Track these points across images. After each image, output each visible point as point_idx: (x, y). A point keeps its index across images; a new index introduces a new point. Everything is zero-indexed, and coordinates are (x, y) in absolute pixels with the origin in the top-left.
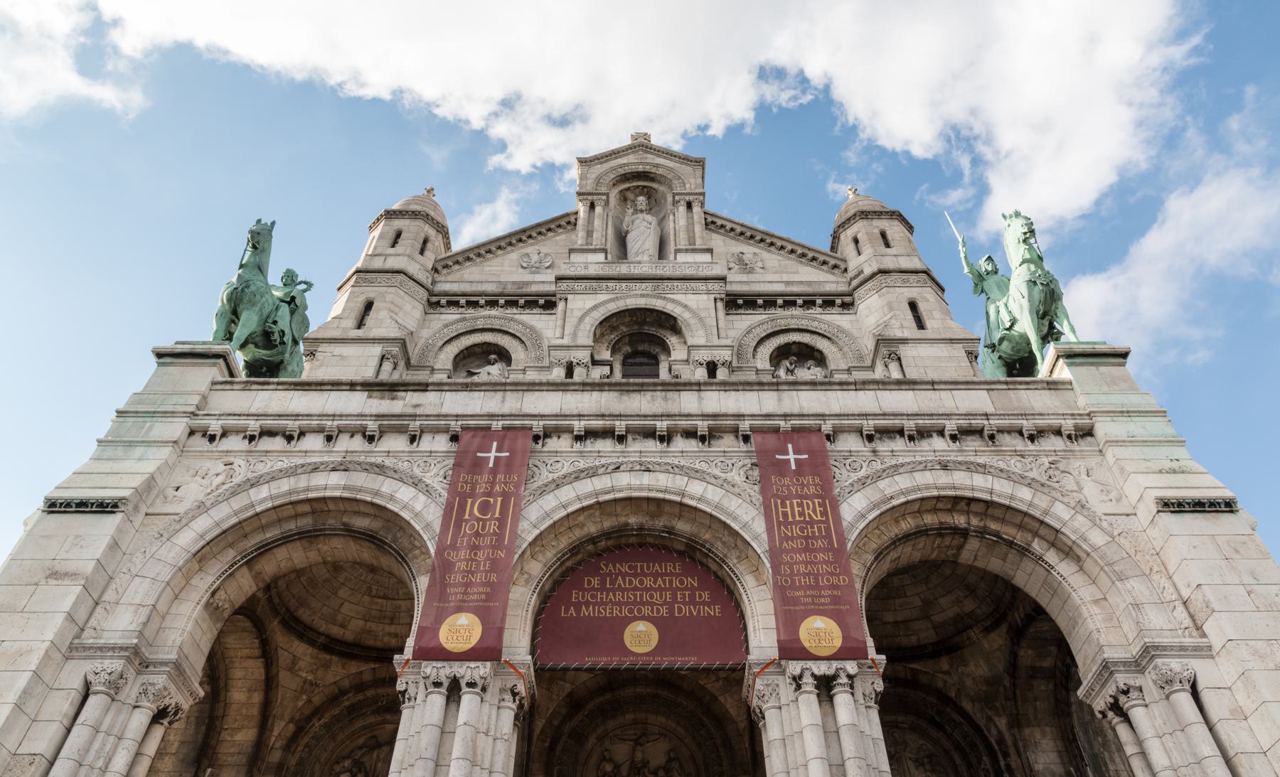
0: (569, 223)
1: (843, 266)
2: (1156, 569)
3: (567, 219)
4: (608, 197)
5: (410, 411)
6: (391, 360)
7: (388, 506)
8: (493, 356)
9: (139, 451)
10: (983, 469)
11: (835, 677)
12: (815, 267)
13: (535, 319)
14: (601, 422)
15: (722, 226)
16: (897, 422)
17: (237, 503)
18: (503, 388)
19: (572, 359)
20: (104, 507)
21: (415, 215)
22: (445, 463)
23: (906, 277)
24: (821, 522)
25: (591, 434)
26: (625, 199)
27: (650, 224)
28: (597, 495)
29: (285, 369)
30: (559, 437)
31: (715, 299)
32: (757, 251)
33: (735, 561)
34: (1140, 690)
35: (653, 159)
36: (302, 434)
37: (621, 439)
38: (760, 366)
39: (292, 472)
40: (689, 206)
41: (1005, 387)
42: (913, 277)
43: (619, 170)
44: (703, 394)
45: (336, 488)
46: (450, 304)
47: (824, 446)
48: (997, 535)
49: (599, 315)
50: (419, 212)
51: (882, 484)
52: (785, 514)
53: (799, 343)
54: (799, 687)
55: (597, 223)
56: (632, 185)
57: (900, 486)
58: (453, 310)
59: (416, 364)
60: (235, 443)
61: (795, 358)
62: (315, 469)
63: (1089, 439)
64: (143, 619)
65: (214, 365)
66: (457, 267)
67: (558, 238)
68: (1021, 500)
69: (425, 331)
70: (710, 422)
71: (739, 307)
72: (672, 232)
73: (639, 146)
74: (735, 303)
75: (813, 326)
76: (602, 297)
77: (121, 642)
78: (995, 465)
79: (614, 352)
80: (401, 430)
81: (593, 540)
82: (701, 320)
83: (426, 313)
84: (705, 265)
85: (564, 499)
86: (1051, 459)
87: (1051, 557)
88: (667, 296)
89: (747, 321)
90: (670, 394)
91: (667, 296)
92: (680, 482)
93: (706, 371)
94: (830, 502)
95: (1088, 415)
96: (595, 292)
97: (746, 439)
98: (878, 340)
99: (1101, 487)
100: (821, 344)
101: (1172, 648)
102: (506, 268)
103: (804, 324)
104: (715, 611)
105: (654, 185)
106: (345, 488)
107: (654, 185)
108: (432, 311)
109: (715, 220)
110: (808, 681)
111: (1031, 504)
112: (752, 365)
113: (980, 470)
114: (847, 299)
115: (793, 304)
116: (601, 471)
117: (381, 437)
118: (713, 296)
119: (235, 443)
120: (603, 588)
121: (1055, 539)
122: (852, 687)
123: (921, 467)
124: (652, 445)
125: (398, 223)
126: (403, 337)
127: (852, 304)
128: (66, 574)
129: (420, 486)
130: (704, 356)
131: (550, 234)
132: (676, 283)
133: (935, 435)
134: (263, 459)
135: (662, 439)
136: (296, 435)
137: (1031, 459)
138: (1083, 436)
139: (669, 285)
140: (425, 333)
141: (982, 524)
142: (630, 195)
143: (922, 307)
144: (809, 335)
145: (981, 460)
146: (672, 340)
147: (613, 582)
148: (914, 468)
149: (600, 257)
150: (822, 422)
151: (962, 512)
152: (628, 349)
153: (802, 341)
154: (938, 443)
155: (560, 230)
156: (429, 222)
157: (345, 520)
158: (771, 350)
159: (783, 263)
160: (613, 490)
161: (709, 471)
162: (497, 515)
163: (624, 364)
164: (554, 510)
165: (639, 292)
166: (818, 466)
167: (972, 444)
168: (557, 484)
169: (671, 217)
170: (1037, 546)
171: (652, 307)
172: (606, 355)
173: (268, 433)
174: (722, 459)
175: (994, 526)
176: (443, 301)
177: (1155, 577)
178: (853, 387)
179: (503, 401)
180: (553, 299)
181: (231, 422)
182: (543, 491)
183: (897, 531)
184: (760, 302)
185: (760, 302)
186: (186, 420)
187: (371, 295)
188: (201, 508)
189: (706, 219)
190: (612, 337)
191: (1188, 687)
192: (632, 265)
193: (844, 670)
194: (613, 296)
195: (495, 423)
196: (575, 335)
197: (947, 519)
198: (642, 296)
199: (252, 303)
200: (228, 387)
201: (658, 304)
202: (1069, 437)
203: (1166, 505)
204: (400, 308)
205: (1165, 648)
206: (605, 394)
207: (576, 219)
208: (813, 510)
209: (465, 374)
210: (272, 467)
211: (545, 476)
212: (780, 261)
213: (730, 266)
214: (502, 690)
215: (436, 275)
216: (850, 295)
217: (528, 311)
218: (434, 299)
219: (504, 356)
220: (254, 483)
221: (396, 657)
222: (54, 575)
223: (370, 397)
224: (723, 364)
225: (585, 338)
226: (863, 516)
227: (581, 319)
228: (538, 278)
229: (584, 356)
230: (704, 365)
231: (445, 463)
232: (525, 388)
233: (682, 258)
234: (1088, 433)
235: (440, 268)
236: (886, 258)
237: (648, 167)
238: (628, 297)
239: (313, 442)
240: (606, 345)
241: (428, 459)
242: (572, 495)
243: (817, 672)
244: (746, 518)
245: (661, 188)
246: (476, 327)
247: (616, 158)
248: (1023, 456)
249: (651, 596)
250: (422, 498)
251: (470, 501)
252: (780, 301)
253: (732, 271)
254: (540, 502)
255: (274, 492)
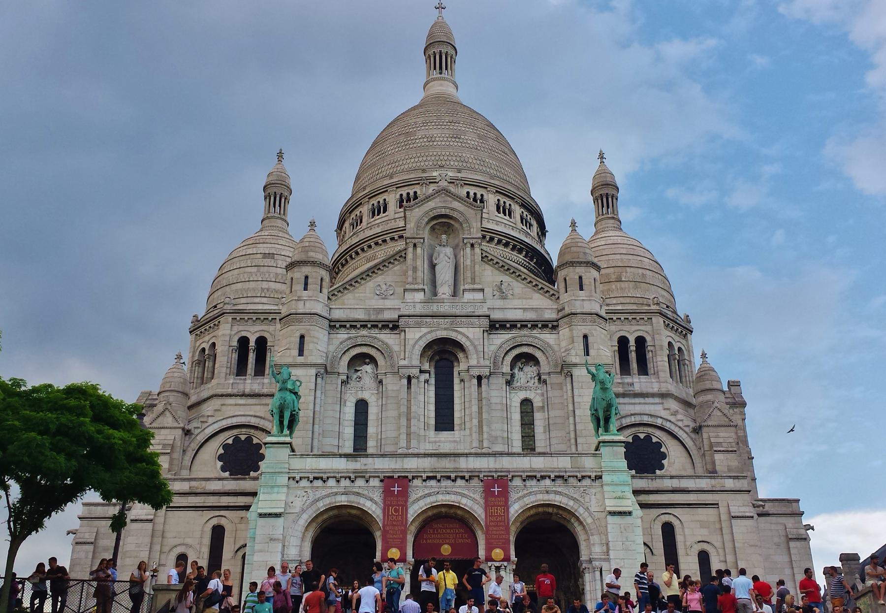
0: (401, 256)
1: (557, 296)
2: (603, 532)
3: (399, 255)
4: (424, 241)
5: (363, 467)
6: (321, 376)
7: (364, 508)
8: (367, 360)
9: (276, 490)
10: (560, 493)
11: (501, 566)
12: (541, 294)
13: (387, 338)
14: (432, 474)
15: (492, 260)
16: (534, 474)
17: (314, 508)
18: (395, 456)
19: (411, 374)
20: (277, 515)
21: (314, 263)
22: (380, 490)
23: (584, 318)
24: (503, 516)
25: (429, 478)
26: (434, 229)
27: (449, 259)
28: (431, 503)
29: (295, 421)
30: (417, 479)
31: (483, 331)
32: (510, 279)
33: (476, 525)
34: (589, 568)
35: (451, 202)
36: (328, 478)
37: (439, 481)
38: (504, 370)
39: (328, 496)
40: (472, 245)
41: (577, 455)
42: (589, 317)
43: (431, 213)
44: (468, 458)
45: (345, 502)
46: (341, 326)
47: (508, 483)
48: (561, 515)
49: (423, 343)
50: (316, 262)
51: (525, 499)
52: (492, 512)
53: (527, 353)
54: (490, 569)
55: (419, 263)
56: (438, 221)
57: (531, 501)
58: (343, 330)
59: (330, 371)
60: (304, 483)
61: (524, 360)
62: (336, 494)
63: (600, 480)
64: (298, 551)
65: (287, 447)
66: (340, 294)
67: (395, 268)
68: (569, 506)
69: (331, 346)
70: (470, 474)
71: (497, 329)
72: (462, 267)
73: (442, 190)
74: (495, 326)
75: (535, 342)
76: (424, 330)
77: (296, 559)
78: (564, 492)
79: (430, 361)
80: (364, 477)
81: (430, 517)
82: (475, 347)
83: (329, 334)
84: (479, 304)
85: (421, 506)
86: (584, 489)
87: (576, 524)
88: (458, 329)
89: (501, 338)
90: (457, 459)
91: (458, 329)
92: (459, 498)
93: (476, 380)
94: (506, 507)
95: (601, 471)
96: (419, 326)
97: (482, 481)
98: (563, 364)
99: (597, 501)
100: (538, 354)
101: (598, 559)
102: (368, 295)
103: (529, 341)
104: (469, 541)
105: (452, 222)
106: (348, 501)
107: (452, 222)
108: (332, 332)
109: (488, 255)
110: (493, 567)
111: (572, 507)
112: (500, 371)
113: (559, 494)
114: (555, 323)
115: (526, 326)
116: (432, 494)
117: (355, 479)
118: (482, 329)
119: (304, 483)
120: (434, 533)
121: (578, 519)
122: (505, 569)
123: (540, 492)
124: (449, 483)
125: (307, 270)
126: (325, 364)
127: (558, 326)
128: (275, 539)
129: (373, 501)
130: (475, 372)
131: (391, 266)
132: (464, 319)
133: (547, 478)
134: (317, 490)
135: (453, 481)
136: (326, 480)
137: (578, 488)
138: (598, 479)
139: (459, 320)
140: (332, 348)
141: (557, 512)
142: (437, 227)
143: (590, 339)
144: (532, 347)
145: (560, 490)
146: (461, 355)
147: (437, 531)
148: (536, 493)
149: (420, 296)
150: (508, 474)
151: (551, 507)
152: (437, 358)
153: (528, 352)
154: (547, 482)
155: (396, 263)
156: (322, 266)
157: (348, 511)
158: (511, 358)
159: (524, 290)
160: (437, 501)
161: (468, 494)
162: (400, 514)
163: (436, 368)
164: (418, 510)
165: (443, 326)
166: (505, 493)
167: (559, 482)
168: (418, 500)
169: (462, 252)
170: (572, 520)
171: (450, 337)
172: (426, 366)
173: (316, 478)
174: (473, 488)
175: (561, 512)
176: (337, 326)
177: (601, 535)
178: (523, 455)
179: (396, 462)
180: (397, 323)
181: (303, 475)
182: (414, 502)
183: (529, 514)
184: (508, 325)
185: (508, 325)
186: (287, 475)
187: (303, 332)
188: (303, 511)
189: (482, 254)
190: (430, 353)
191: (599, 570)
192: (439, 304)
193: (504, 565)
194: (429, 329)
195: (395, 475)
196: (411, 358)
197: (546, 509)
198: (445, 329)
199: (288, 408)
200: (295, 456)
201: (453, 335)
202: (593, 480)
203: (610, 513)
204: (318, 339)
205: (596, 559)
206: (433, 458)
207: (405, 254)
208: (500, 510)
209: (354, 371)
210: (321, 493)
211: (413, 497)
212: (522, 288)
213: (494, 294)
214: (406, 569)
215: (329, 301)
216: (557, 321)
217: (384, 331)
218: (332, 324)
219: (373, 360)
220: (317, 500)
221: (375, 560)
222: (271, 539)
223: (347, 461)
224: (485, 377)
225: (416, 362)
226: (517, 511)
227: (414, 346)
228: (388, 303)
229: (415, 372)
230: (476, 378)
231: (380, 490)
232: (403, 456)
233: (468, 296)
234: (601, 477)
235: (331, 297)
236: (577, 302)
237: (448, 210)
238: (437, 330)
239: (332, 482)
240: (426, 359)
241: (374, 489)
242: (423, 504)
243: (496, 565)
244: (480, 513)
245: (456, 225)
246: (357, 343)
247: (428, 201)
248: (575, 487)
249: (449, 536)
250: (374, 505)
251: (390, 507)
252: (519, 326)
253: (495, 296)
254: (413, 507)
255: (325, 503)
